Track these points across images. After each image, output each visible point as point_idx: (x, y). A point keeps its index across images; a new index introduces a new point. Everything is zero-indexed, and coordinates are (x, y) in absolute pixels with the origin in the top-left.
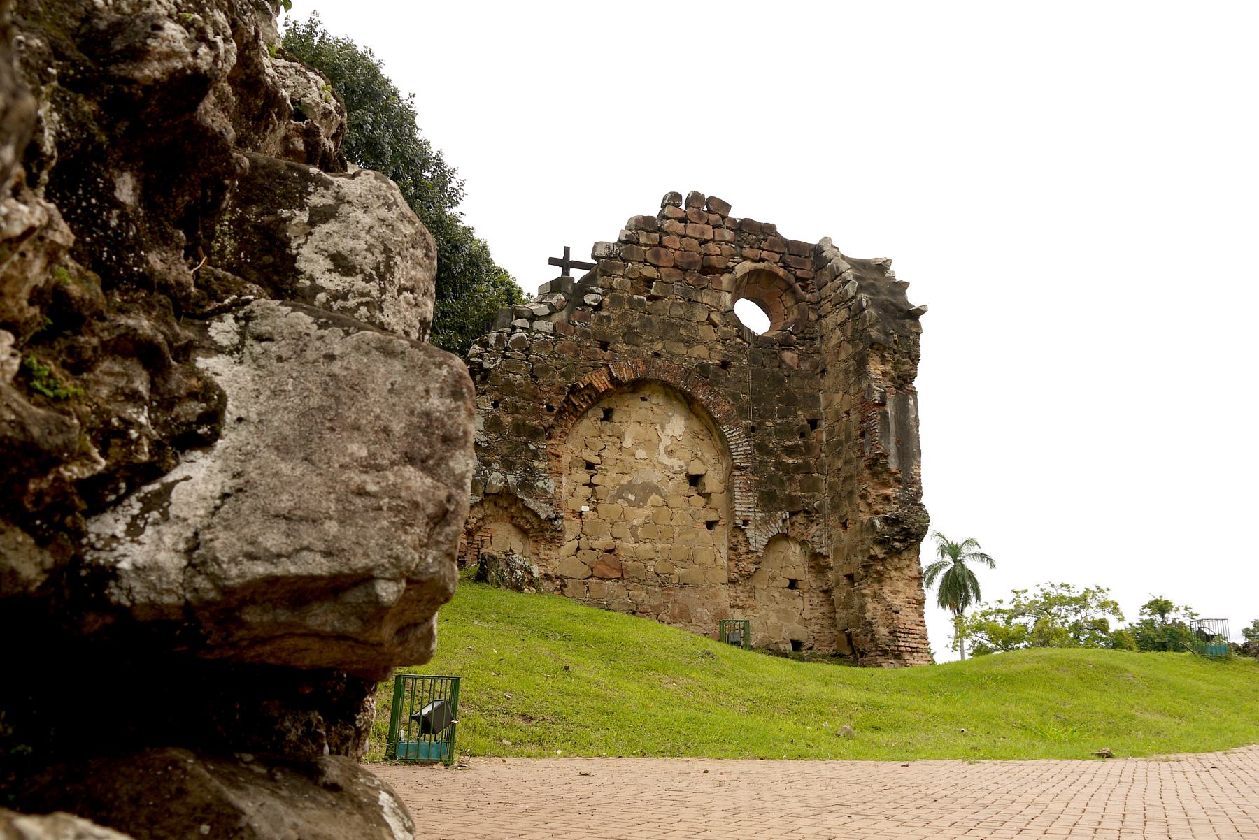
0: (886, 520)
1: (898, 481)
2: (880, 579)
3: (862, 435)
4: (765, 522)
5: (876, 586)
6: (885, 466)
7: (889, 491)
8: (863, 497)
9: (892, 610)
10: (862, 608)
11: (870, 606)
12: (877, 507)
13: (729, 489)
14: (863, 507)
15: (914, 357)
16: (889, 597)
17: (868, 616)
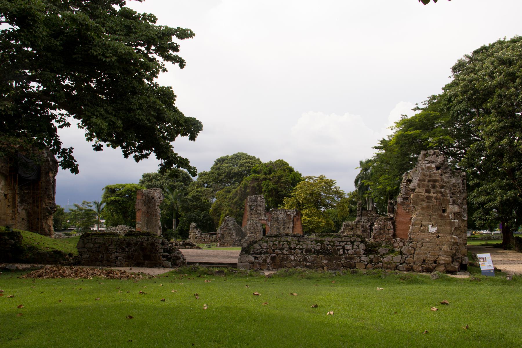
0: (51, 208)
1: (52, 199)
2: (47, 219)
3: (46, 189)
4: (21, 206)
5: (46, 221)
6: (51, 196)
7: (51, 201)
8: (44, 202)
9: (49, 226)
10: (42, 225)
11: (44, 225)
12: (48, 205)
13: (14, 199)
14: (44, 204)
15: (57, 172)
16: (49, 223)
17: (44, 227)
